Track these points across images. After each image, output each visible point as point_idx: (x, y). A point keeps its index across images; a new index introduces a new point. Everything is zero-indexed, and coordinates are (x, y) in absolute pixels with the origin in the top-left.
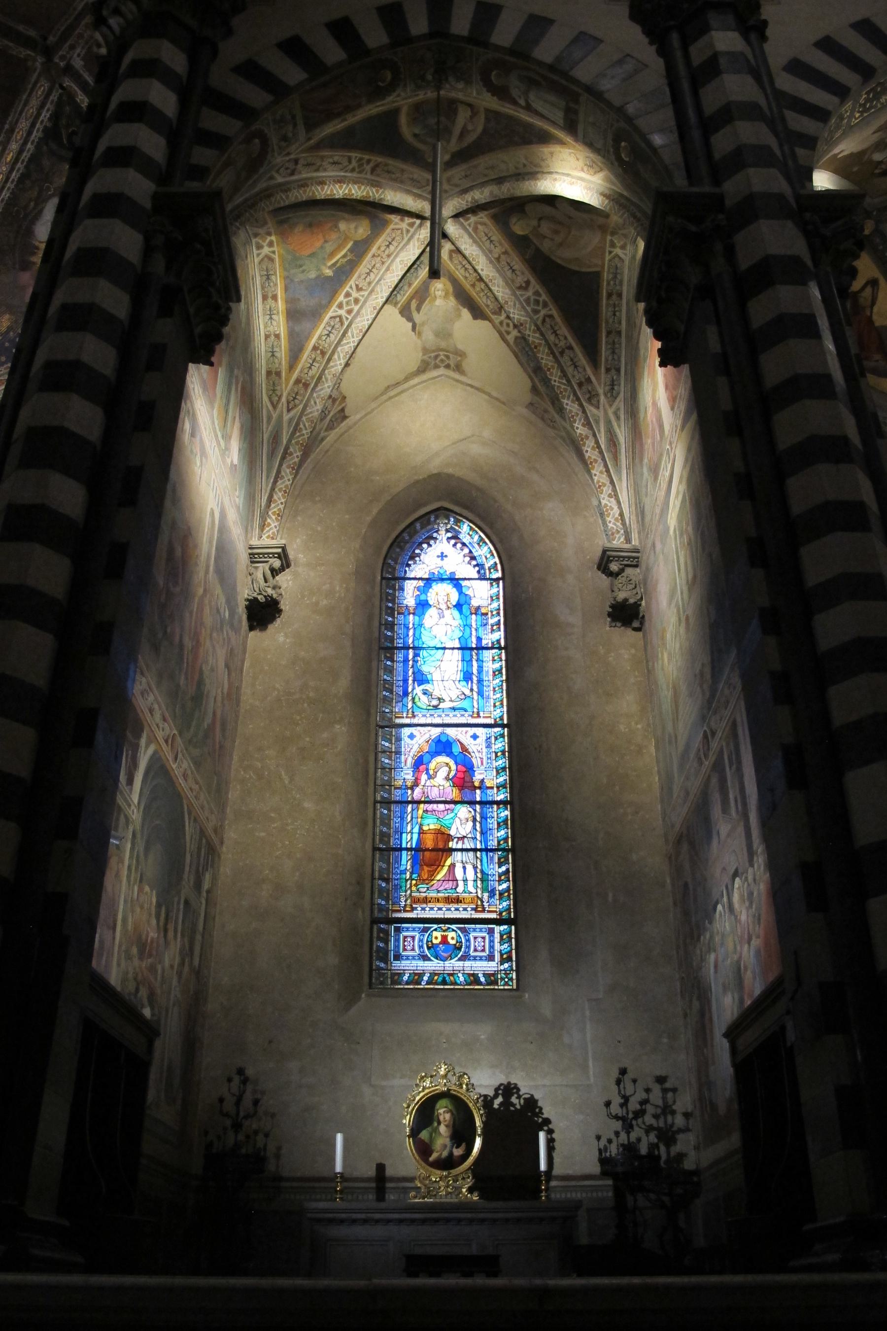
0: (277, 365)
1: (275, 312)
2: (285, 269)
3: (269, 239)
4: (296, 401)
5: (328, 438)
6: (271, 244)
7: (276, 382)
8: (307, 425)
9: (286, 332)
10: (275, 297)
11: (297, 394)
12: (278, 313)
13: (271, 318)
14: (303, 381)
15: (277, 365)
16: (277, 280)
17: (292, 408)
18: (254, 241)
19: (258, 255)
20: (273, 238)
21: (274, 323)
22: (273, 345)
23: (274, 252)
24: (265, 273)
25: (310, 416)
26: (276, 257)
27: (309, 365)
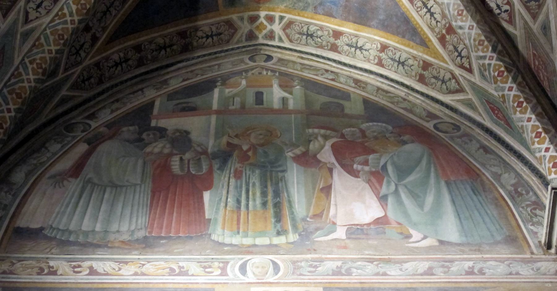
0: (416, 63)
1: (354, 40)
2: (304, 9)
3: (262, 20)
4: (463, 54)
5: (552, 17)
6: (271, 19)
7: (435, 73)
8: (481, 54)
9: (382, 33)
10: (337, 34)
11: (456, 49)
12: (356, 36)
13: (361, 48)
14: (444, 32)
15: (416, 63)
16: (316, 25)
17: (470, 65)
18: (261, 41)
19: (281, 40)
20: (263, 14)
21: (367, 46)
22: (392, 59)
23: (282, 18)
24: (304, 37)
25: (472, 41)
26: (288, 16)
27: (428, 15)
